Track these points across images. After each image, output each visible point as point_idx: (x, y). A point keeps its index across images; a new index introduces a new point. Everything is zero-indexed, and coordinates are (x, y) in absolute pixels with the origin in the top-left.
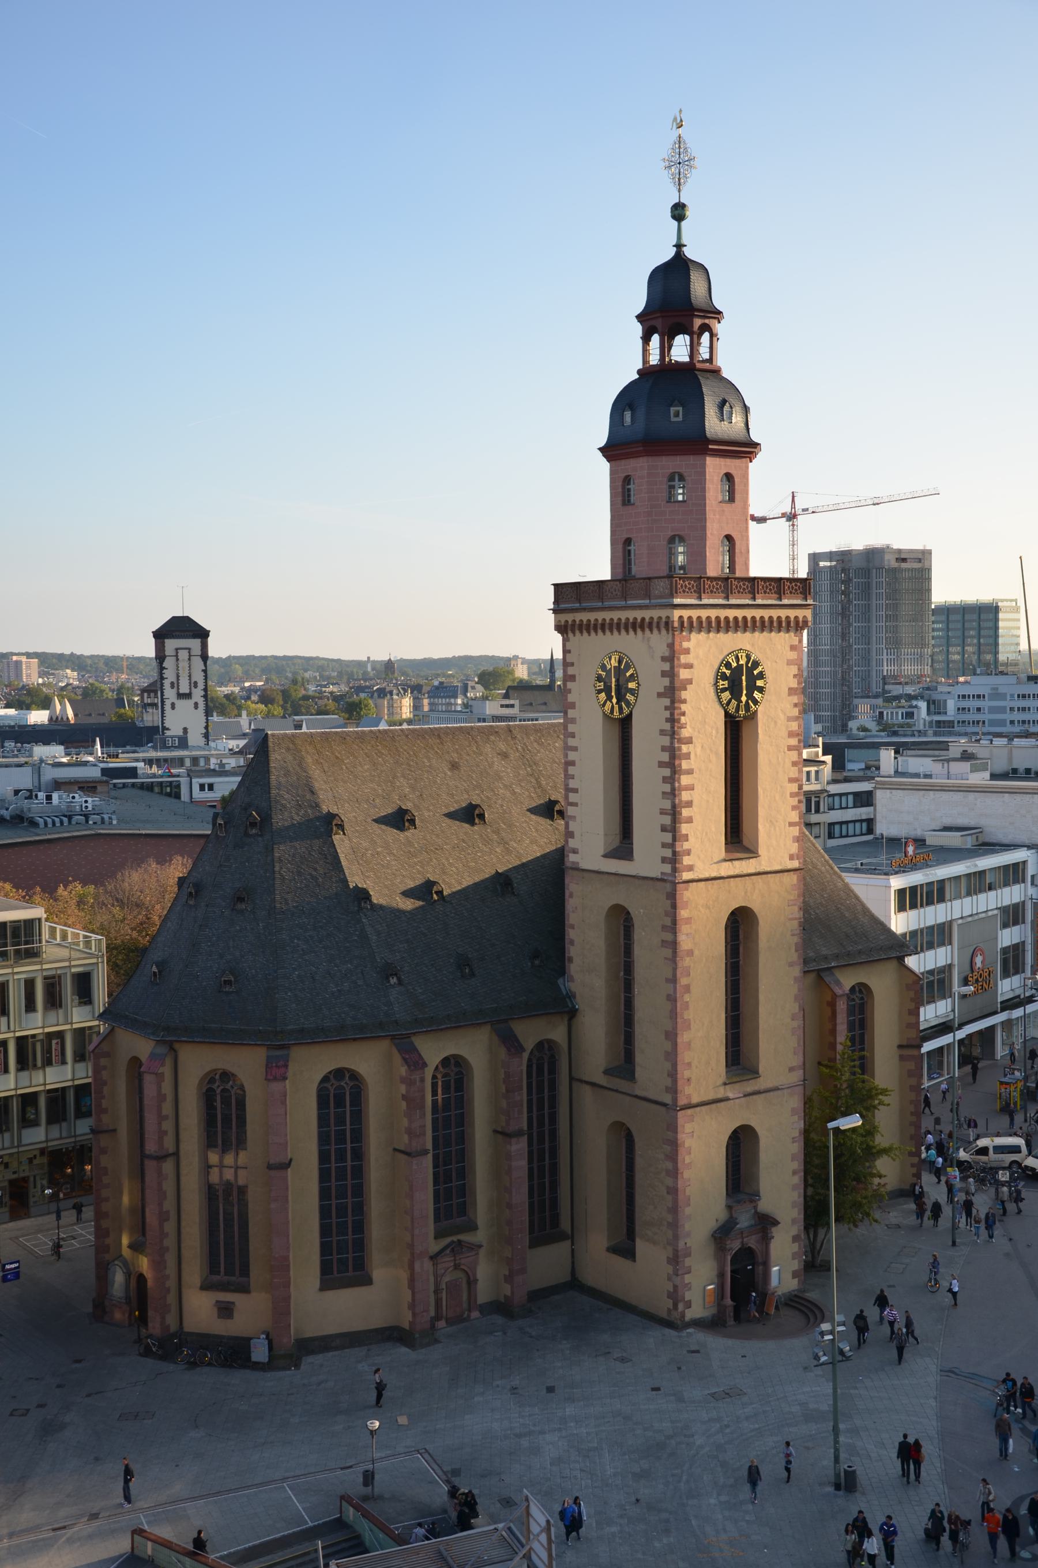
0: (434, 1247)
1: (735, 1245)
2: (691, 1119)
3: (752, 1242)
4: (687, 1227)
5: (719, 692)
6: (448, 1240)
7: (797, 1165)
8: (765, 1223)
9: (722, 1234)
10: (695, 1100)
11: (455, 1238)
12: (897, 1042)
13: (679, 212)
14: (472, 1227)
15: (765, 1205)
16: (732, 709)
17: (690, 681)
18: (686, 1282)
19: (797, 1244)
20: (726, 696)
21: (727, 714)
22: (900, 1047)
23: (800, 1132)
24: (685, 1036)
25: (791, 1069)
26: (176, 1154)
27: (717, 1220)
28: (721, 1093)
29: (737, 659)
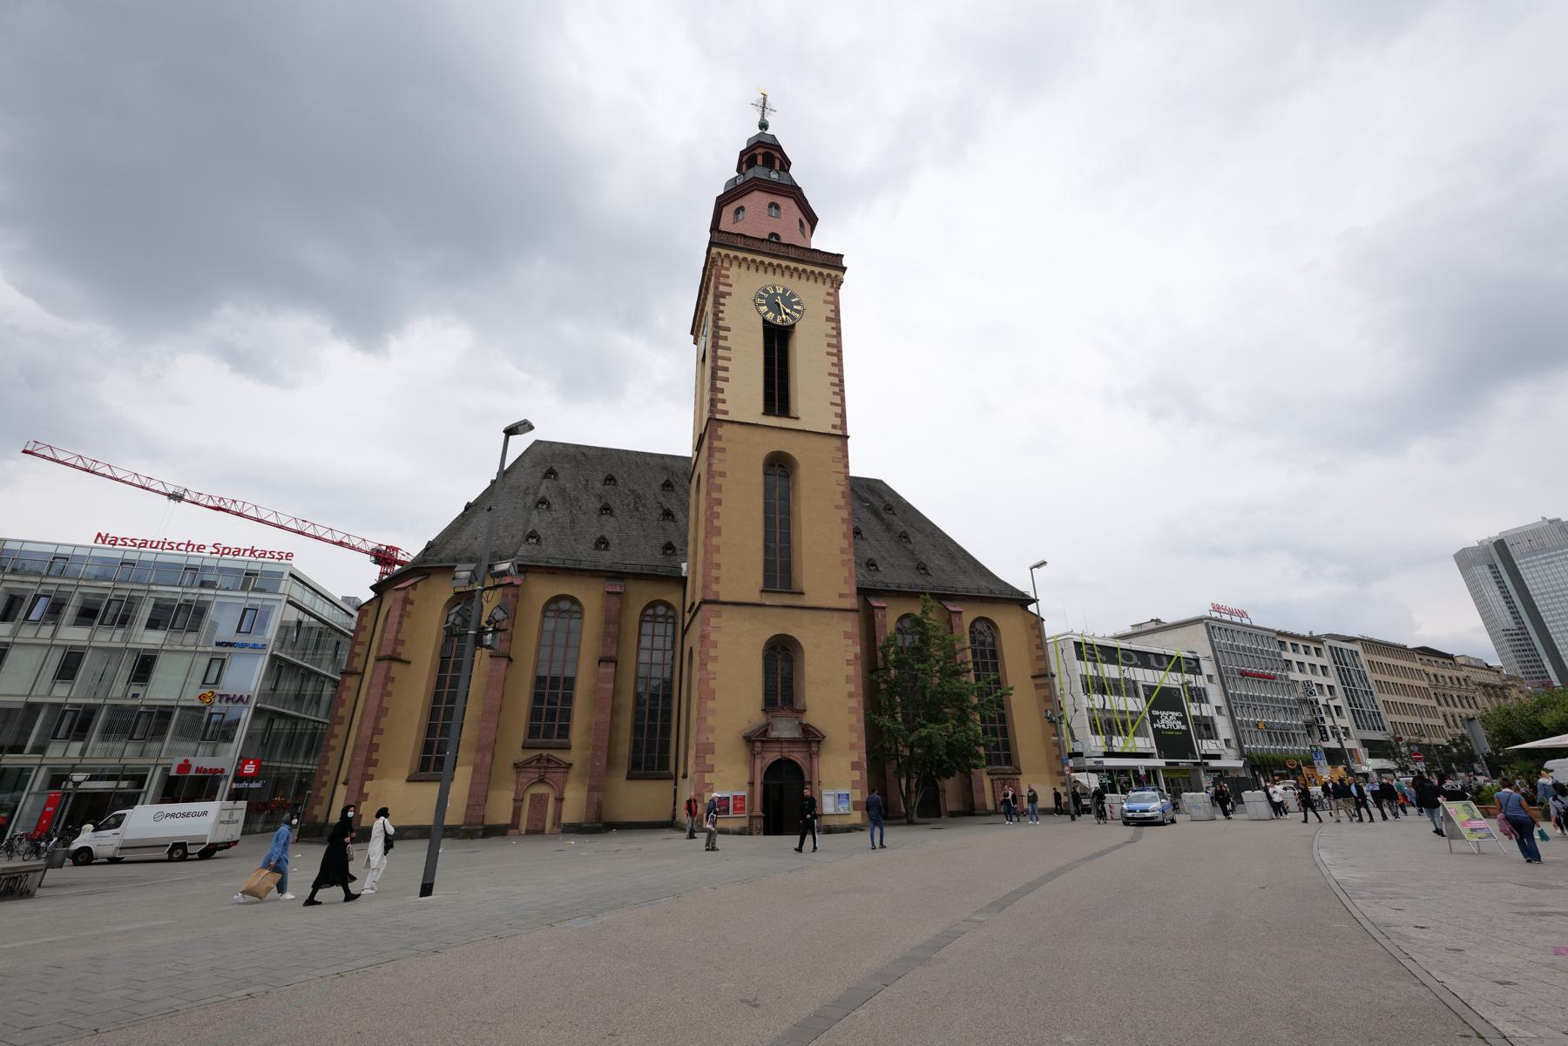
1: (772, 756)
2: (718, 614)
3: (798, 756)
4: (710, 721)
5: (758, 305)
6: (538, 752)
7: (856, 687)
8: (811, 738)
9: (756, 740)
10: (722, 599)
11: (545, 753)
12: (1030, 673)
13: (763, 126)
14: (568, 748)
15: (814, 717)
16: (770, 316)
17: (730, 294)
18: (707, 781)
19: (858, 773)
20: (764, 309)
21: (765, 321)
22: (1034, 677)
23: (856, 656)
25: (841, 596)
26: (362, 675)
27: (749, 722)
28: (756, 597)
29: (774, 289)
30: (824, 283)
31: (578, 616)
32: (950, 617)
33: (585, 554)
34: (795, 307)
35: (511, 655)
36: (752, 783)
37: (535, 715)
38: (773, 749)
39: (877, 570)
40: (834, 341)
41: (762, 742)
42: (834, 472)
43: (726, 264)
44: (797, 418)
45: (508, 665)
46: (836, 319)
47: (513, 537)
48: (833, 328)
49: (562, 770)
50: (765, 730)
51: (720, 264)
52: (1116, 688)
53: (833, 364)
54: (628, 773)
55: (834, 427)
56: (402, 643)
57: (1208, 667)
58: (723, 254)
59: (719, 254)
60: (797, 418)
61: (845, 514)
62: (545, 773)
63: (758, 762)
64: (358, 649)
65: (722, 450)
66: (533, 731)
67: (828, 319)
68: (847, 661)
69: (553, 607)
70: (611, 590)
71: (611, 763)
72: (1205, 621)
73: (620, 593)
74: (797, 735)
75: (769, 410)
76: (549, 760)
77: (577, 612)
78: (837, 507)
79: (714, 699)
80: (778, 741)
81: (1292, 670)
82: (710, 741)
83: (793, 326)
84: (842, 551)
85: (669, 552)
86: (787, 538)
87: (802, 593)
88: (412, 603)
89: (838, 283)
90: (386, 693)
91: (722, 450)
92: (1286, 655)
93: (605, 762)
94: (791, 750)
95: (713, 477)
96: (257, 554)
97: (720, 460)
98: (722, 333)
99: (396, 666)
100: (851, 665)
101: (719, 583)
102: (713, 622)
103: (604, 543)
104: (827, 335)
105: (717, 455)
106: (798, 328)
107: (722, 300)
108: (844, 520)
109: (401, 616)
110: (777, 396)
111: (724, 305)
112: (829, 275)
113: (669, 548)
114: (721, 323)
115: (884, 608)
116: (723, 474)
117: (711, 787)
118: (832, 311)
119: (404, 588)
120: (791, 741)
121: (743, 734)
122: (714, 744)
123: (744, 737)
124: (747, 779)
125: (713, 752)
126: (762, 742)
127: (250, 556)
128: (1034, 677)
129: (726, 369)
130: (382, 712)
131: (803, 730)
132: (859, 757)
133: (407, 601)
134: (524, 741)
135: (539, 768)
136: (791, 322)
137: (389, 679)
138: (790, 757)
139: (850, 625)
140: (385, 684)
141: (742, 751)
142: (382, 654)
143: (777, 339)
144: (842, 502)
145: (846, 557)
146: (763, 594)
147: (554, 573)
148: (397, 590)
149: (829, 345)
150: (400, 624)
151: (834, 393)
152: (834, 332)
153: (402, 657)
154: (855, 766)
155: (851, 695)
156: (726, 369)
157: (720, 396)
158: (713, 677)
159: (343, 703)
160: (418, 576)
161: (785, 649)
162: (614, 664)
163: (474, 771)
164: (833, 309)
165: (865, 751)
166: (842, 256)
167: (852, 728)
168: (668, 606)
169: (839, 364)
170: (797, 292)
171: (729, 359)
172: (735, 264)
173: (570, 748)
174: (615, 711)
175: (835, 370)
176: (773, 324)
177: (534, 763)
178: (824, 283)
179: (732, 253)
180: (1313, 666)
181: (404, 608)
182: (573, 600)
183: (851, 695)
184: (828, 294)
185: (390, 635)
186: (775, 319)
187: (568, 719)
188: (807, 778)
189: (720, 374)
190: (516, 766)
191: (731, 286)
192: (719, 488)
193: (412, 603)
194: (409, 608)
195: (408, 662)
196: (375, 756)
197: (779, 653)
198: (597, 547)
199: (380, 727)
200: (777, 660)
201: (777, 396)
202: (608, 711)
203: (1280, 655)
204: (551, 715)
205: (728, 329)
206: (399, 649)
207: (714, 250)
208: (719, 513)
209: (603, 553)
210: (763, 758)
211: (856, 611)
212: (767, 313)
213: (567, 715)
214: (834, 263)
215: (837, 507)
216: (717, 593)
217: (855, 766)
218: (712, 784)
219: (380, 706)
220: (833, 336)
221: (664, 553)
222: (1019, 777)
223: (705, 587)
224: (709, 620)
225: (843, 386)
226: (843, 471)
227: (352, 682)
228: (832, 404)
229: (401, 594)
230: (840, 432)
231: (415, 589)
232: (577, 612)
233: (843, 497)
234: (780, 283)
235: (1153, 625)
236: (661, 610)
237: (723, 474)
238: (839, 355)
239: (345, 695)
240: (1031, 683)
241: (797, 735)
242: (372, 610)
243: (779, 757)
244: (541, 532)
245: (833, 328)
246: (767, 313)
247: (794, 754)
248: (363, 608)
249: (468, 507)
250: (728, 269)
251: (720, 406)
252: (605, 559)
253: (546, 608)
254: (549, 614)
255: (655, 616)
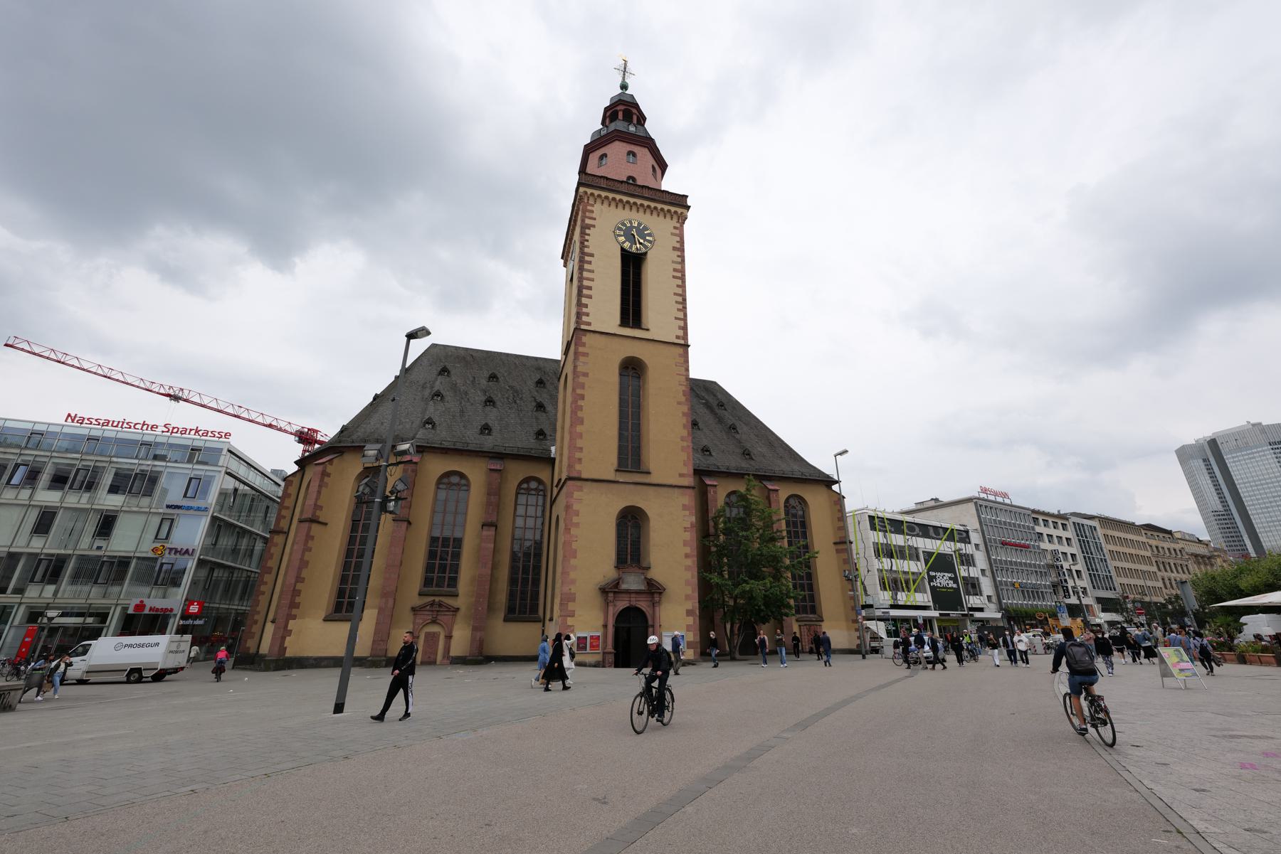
0: (419, 601)
1: (622, 604)
2: (580, 489)
3: (643, 605)
4: (572, 575)
6: (431, 599)
7: (691, 549)
8: (654, 590)
9: (609, 591)
10: (584, 476)
11: (437, 599)
12: (833, 541)
15: (657, 573)
16: (627, 245)
17: (594, 226)
18: (569, 623)
20: (622, 239)
21: (623, 249)
22: (835, 543)
23: (692, 524)
24: (577, 429)
25: (681, 475)
26: (287, 533)
28: (611, 475)
29: (631, 222)
30: (672, 219)
31: (465, 488)
32: (769, 494)
33: (472, 437)
34: (647, 238)
35: (410, 520)
36: (605, 626)
37: (429, 568)
38: (621, 599)
39: (711, 455)
40: (679, 267)
41: (615, 592)
42: (677, 374)
43: (591, 201)
44: (648, 330)
45: (407, 528)
46: (680, 249)
47: (412, 423)
48: (678, 256)
49: (451, 613)
50: (617, 583)
51: (586, 201)
52: (901, 553)
53: (678, 286)
54: (505, 616)
55: (678, 337)
56: (321, 508)
57: (975, 538)
58: (589, 193)
59: (586, 193)
60: (648, 330)
61: (685, 409)
62: (437, 615)
63: (611, 609)
64: (284, 512)
65: (586, 355)
66: (427, 582)
67: (674, 249)
68: (685, 528)
69: (445, 480)
70: (493, 468)
71: (491, 608)
72: (975, 501)
73: (500, 470)
74: (642, 587)
75: (624, 322)
76: (440, 605)
77: (465, 485)
78: (679, 403)
79: (575, 557)
80: (628, 592)
81: (1043, 541)
82: (573, 591)
83: (646, 253)
84: (683, 439)
85: (541, 437)
86: (637, 427)
87: (649, 473)
88: (329, 475)
89: (682, 219)
90: (307, 549)
91: (586, 355)
92: (1038, 529)
93: (486, 607)
94: (637, 599)
95: (578, 377)
96: (200, 433)
97: (584, 363)
98: (587, 258)
99: (315, 527)
100: (688, 531)
101: (581, 463)
102: (576, 494)
103: (487, 429)
104: (673, 262)
105: (582, 359)
106: (649, 255)
107: (587, 231)
108: (684, 414)
109: (320, 486)
110: (632, 311)
111: (589, 235)
112: (676, 212)
113: (540, 434)
114: (586, 250)
115: (716, 486)
116: (586, 375)
117: (572, 628)
118: (678, 242)
119: (323, 463)
120: (638, 592)
121: (599, 586)
122: (575, 594)
123: (600, 589)
124: (601, 622)
125: (574, 600)
126: (615, 592)
127: (195, 434)
128: (835, 543)
129: (590, 288)
130: (304, 564)
131: (648, 583)
132: (693, 606)
133: (325, 474)
134: (420, 590)
135: (432, 611)
136: (643, 250)
137: (309, 537)
138: (637, 606)
139: (688, 499)
140: (306, 542)
141: (598, 600)
142: (305, 516)
143: (632, 264)
144: (683, 399)
145: (685, 444)
146: (617, 473)
147: (446, 453)
148: (316, 464)
149: (675, 270)
150: (319, 492)
151: (679, 310)
152: (679, 260)
153: (320, 520)
154: (689, 613)
155: (687, 556)
156: (590, 288)
157: (584, 310)
158: (575, 539)
159: (271, 557)
160: (335, 453)
161: (634, 517)
162: (494, 528)
163: (379, 612)
164: (679, 240)
165: (697, 601)
166: (687, 196)
167: (687, 583)
168: (540, 481)
169: (683, 286)
170: (649, 225)
171: (592, 280)
172: (599, 201)
173: (457, 596)
174: (494, 567)
175: (679, 291)
176: (630, 252)
177: (428, 607)
178: (672, 219)
179: (596, 192)
180: (1060, 538)
181: (322, 480)
182: (462, 475)
183: (687, 556)
184: (675, 228)
185: (310, 502)
186: (631, 247)
187: (456, 572)
188: (650, 623)
189: (585, 292)
190: (413, 609)
191: (595, 219)
192: (582, 386)
193: (329, 475)
194: (326, 479)
195: (326, 524)
196: (297, 600)
197: (630, 521)
198: (482, 433)
199: (302, 576)
200: (627, 527)
201: (632, 311)
202: (490, 566)
203: (1033, 529)
204: (443, 568)
205: (592, 255)
206: (318, 513)
207: (582, 190)
208: (582, 406)
209: (487, 437)
210: (615, 606)
211: (693, 488)
212: (624, 242)
213: (456, 569)
214: (680, 202)
215: (679, 403)
216: (580, 472)
217: (689, 613)
218: (573, 626)
219: (302, 559)
220: (679, 263)
221: (537, 438)
222: (821, 623)
223: (570, 466)
224: (573, 493)
225: (686, 304)
226: (685, 374)
227: (279, 539)
228: (676, 318)
229: (320, 468)
230: (682, 342)
231: (331, 465)
232: (465, 485)
233: (684, 395)
234: (636, 218)
235: (933, 503)
236: (533, 485)
237: (586, 375)
238: (683, 278)
239: (273, 550)
240: (833, 548)
241: (642, 587)
242: (296, 481)
243: (628, 605)
244: (436, 419)
245: (678, 256)
246: (624, 242)
247: (640, 603)
248: (290, 478)
249: (376, 397)
250: (593, 206)
251: (584, 318)
252: (489, 443)
253: (439, 482)
254: (441, 486)
255: (528, 489)
